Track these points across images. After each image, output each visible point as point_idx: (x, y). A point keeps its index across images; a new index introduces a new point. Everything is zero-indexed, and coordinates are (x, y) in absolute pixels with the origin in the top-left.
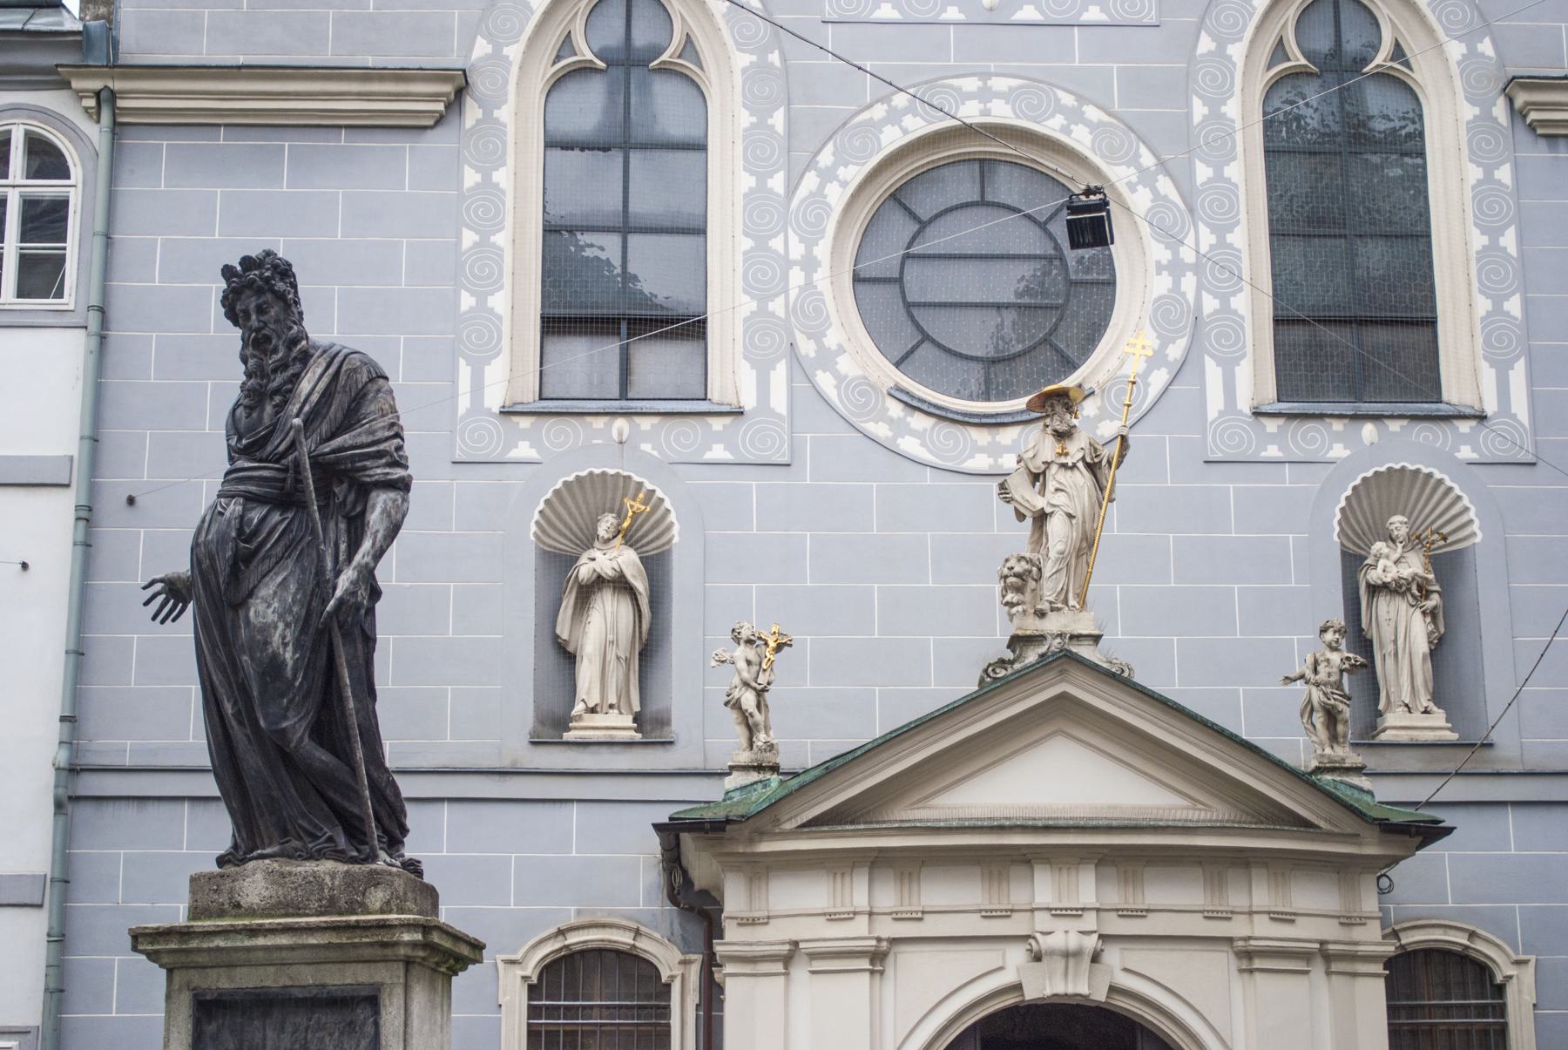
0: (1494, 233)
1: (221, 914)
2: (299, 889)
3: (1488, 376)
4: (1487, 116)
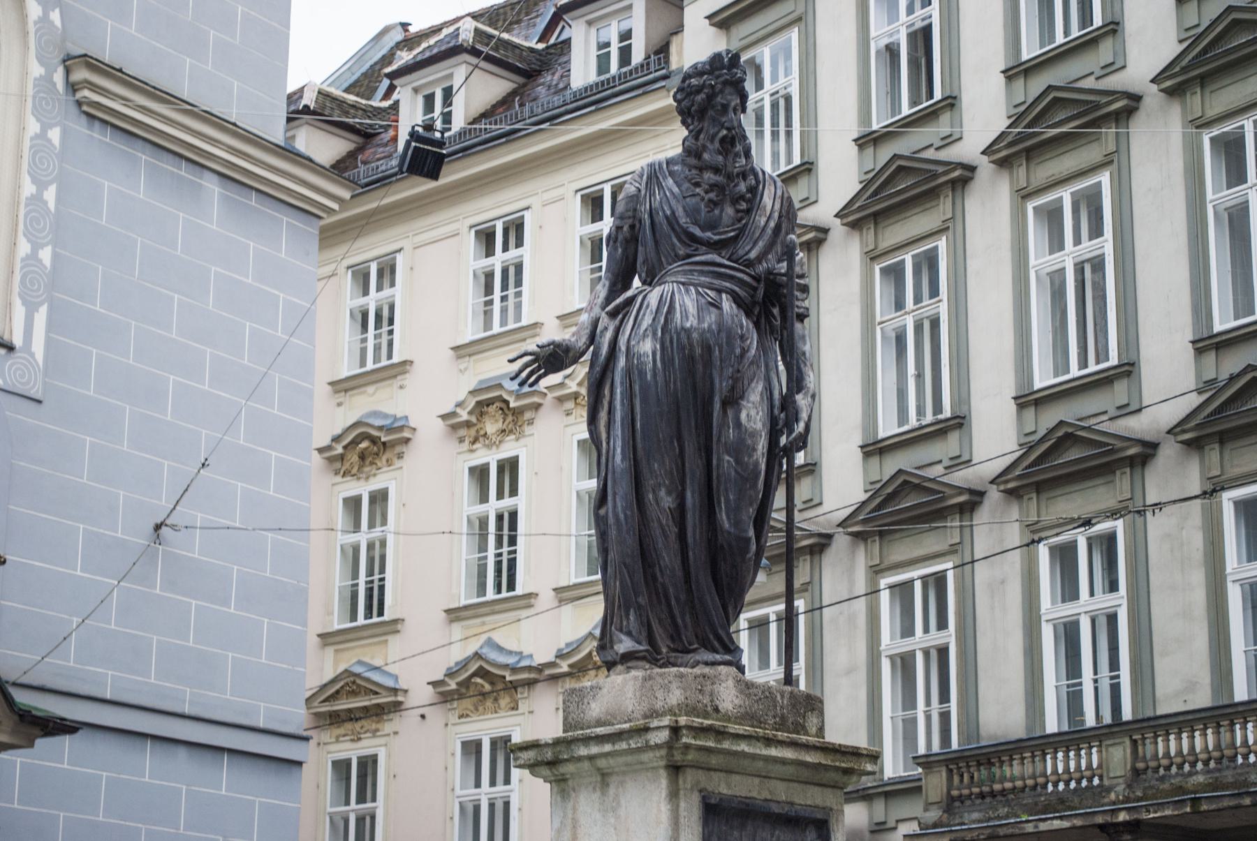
0: (41, 185)
1: (706, 715)
2: (760, 703)
3: (19, 311)
4: (48, 79)
